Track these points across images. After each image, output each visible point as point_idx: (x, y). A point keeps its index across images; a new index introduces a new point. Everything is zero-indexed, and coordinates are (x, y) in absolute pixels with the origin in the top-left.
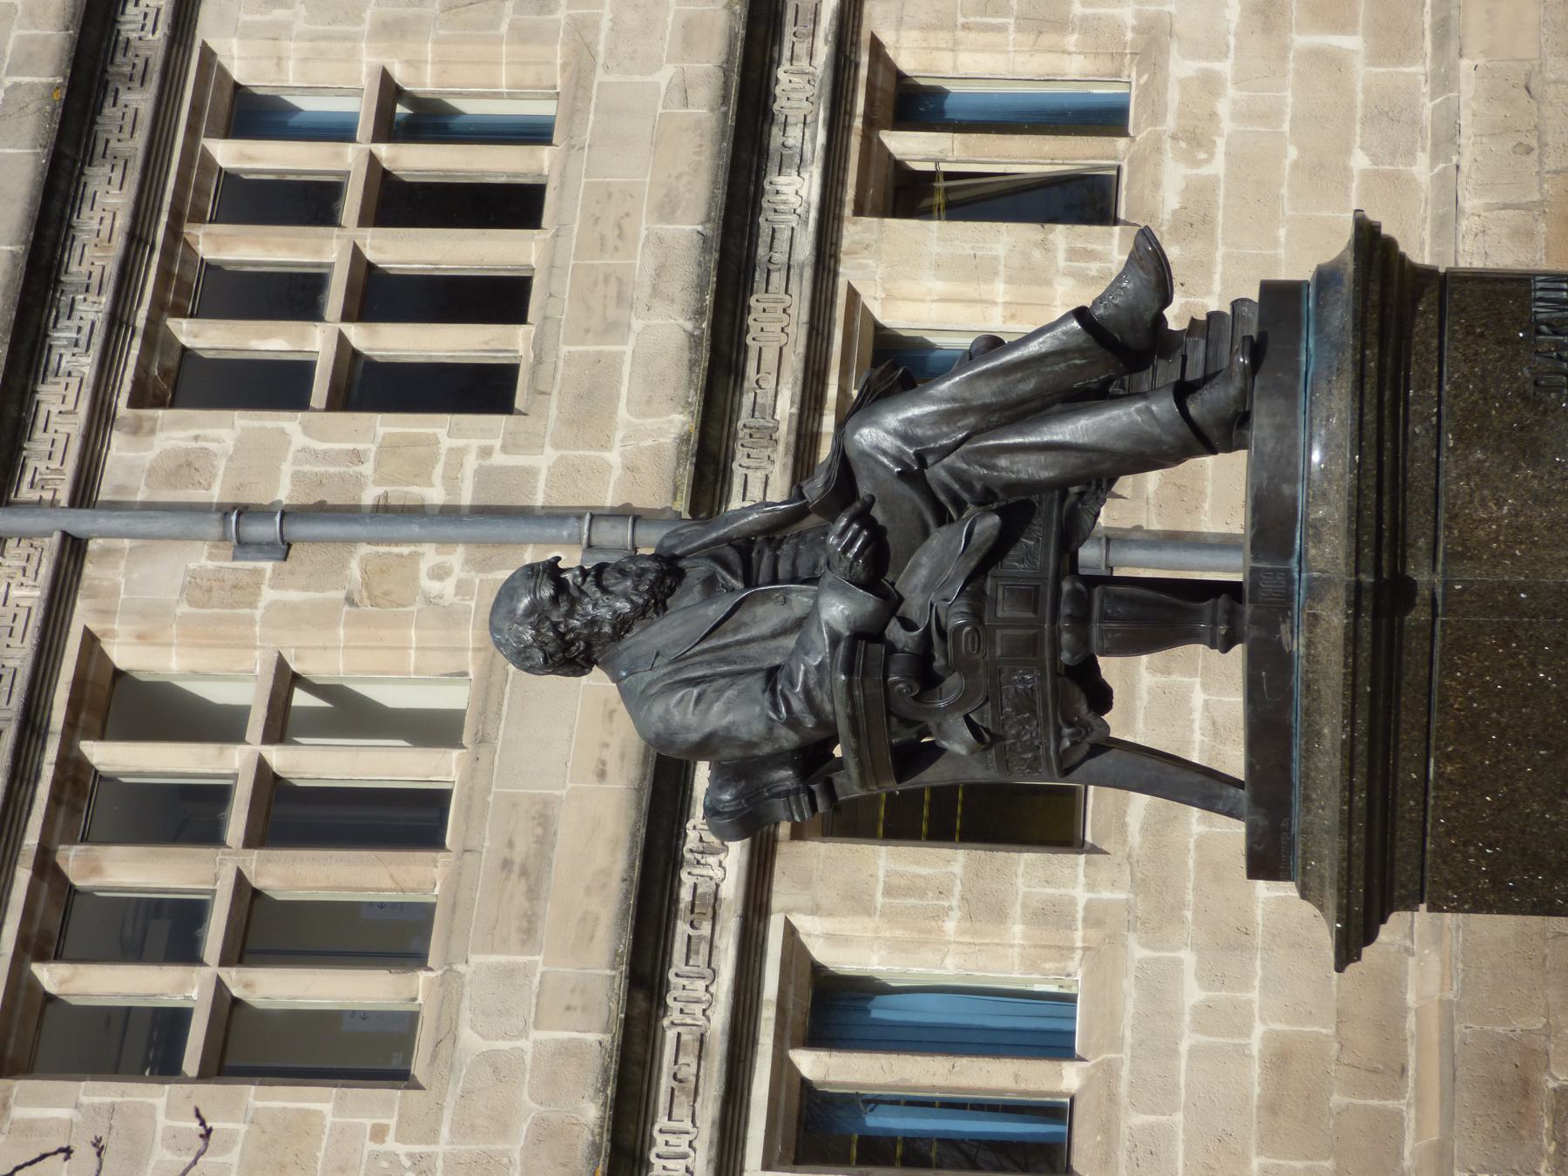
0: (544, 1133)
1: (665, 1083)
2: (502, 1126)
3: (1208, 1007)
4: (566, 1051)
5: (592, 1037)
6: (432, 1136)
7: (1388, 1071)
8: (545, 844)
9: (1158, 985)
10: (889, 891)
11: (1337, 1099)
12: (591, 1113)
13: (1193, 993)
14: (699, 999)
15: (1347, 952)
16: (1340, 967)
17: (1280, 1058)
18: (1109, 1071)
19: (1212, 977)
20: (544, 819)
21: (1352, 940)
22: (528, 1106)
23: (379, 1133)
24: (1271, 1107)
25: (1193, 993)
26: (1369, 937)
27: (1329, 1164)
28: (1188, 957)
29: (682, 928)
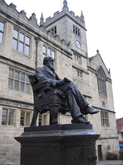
0: (5, 95)
1: (7, 102)
2: (6, 93)
3: (11, 133)
4: (9, 97)
5: (10, 98)
6: (5, 89)
7: (7, 143)
8: (21, 97)
9: (13, 130)
10: (18, 115)
11: (6, 140)
12: (6, 98)
13: (12, 132)
14: (12, 104)
15: (16, 138)
16: (14, 138)
17: (8, 137)
18: (8, 127)
19: (13, 133)
20: (22, 97)
21: (17, 139)
22: (6, 94)
23: (5, 86)
24: (5, 136)
25: (12, 132)
26: (18, 141)
27: (2, 140)
28: (14, 132)
29: (16, 103)
